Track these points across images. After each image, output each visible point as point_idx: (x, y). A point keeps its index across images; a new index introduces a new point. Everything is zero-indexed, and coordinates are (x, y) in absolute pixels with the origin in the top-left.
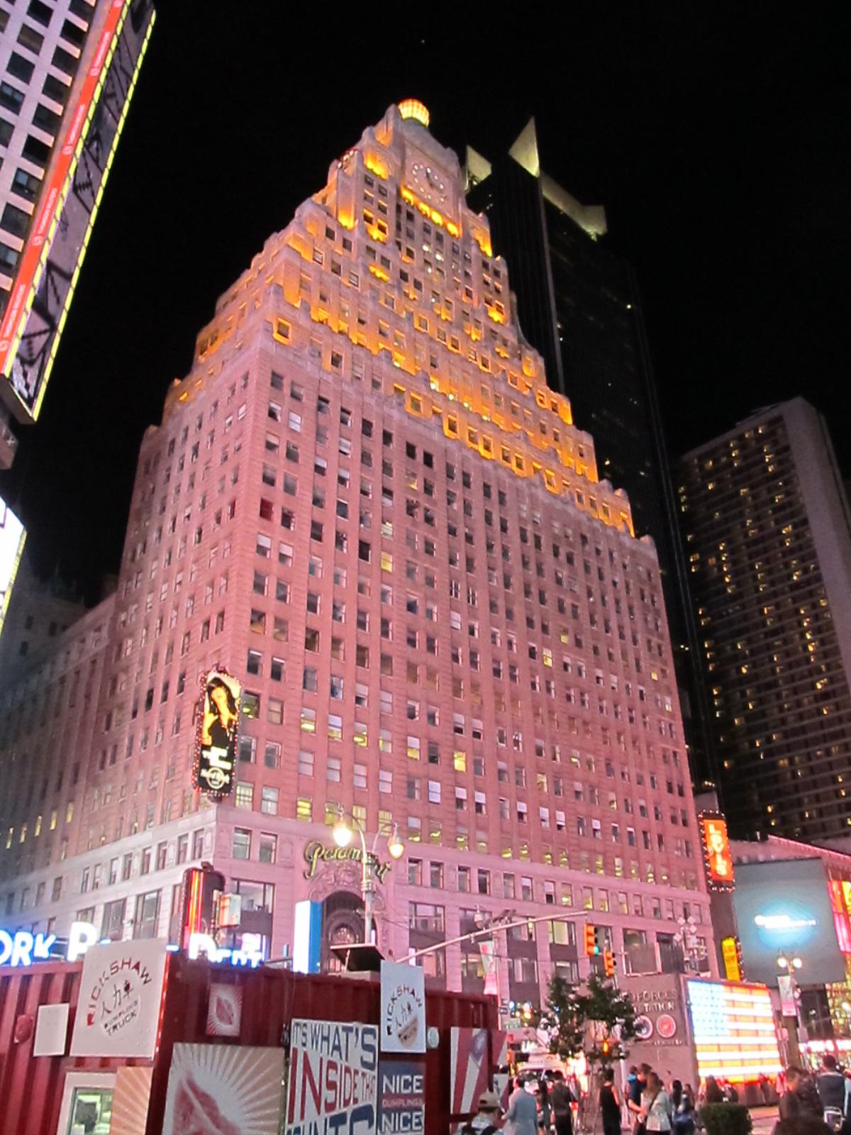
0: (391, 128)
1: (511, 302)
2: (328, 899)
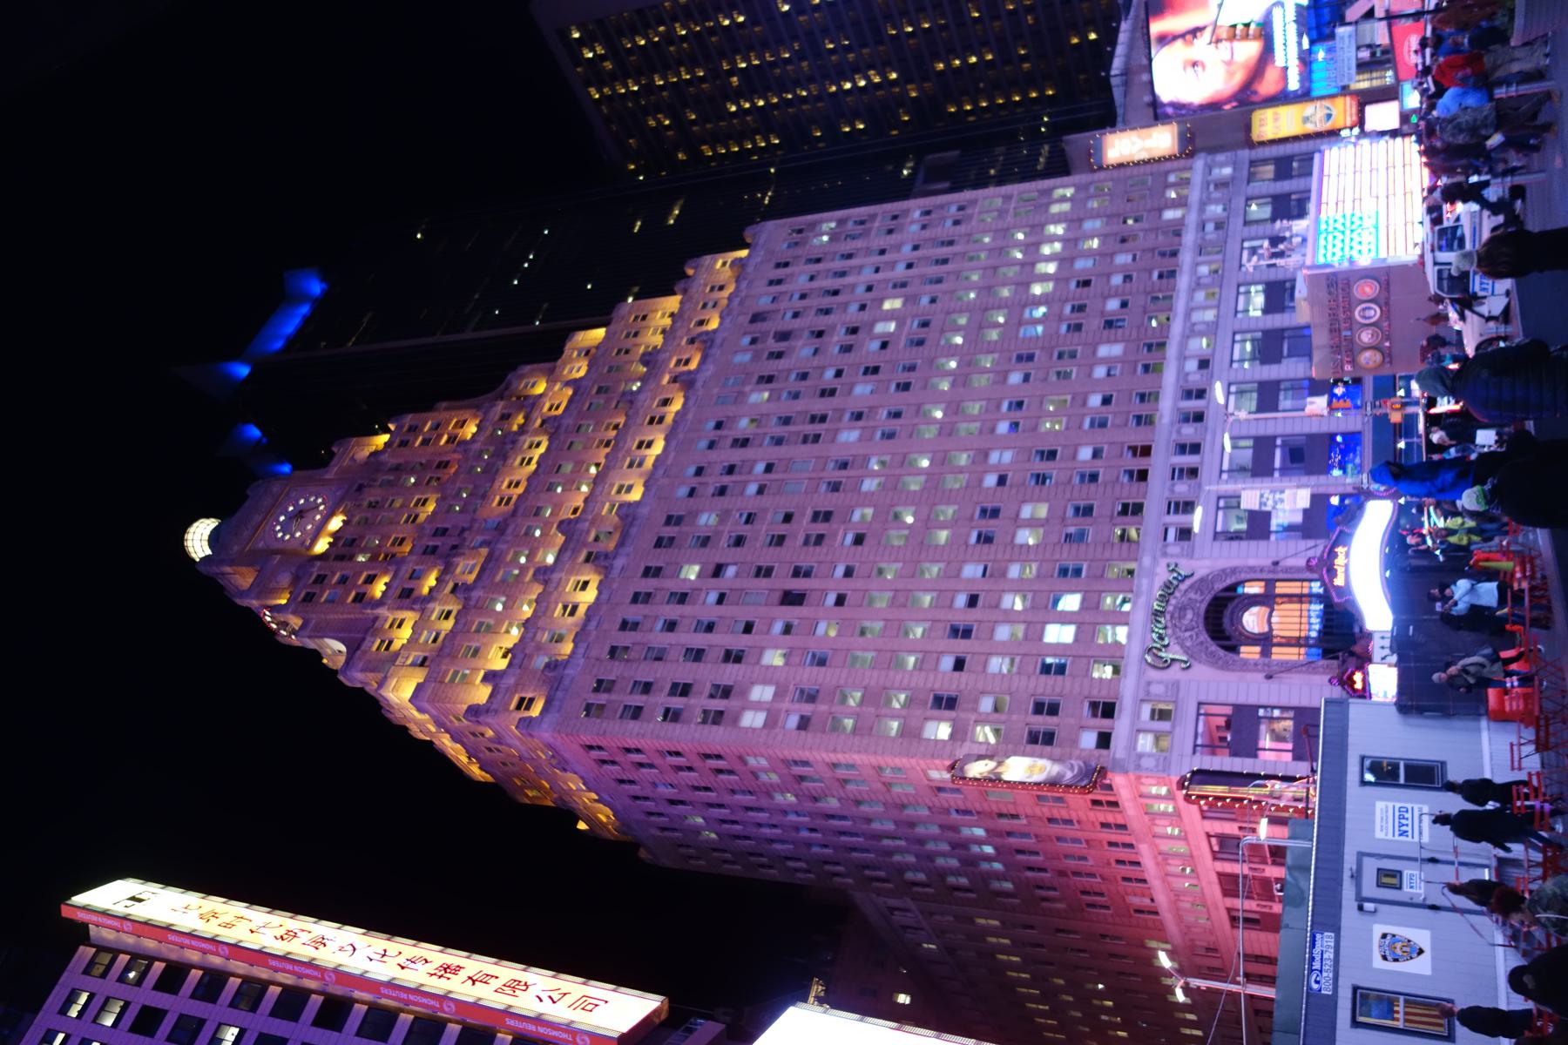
0: (228, 569)
1: (447, 409)
2: (1213, 638)
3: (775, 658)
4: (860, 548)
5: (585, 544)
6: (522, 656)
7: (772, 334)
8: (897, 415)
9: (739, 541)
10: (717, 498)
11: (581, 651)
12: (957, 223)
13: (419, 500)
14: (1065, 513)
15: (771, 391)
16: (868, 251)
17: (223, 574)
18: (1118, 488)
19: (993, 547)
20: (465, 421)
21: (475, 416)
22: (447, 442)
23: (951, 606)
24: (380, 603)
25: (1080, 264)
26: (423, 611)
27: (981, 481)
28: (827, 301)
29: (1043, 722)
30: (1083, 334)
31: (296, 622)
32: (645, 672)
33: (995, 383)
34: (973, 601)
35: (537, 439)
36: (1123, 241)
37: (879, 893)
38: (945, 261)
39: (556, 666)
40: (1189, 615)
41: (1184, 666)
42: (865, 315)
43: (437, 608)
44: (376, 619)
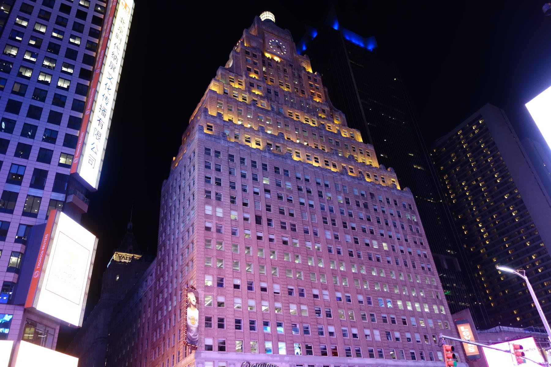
0: (256, 26)
1: (325, 91)
3: (234, 215)
4: (282, 243)
5: (274, 142)
6: (228, 125)
7: (366, 201)
8: (339, 253)
9: (280, 198)
10: (297, 187)
11: (231, 145)
12: (423, 268)
13: (289, 86)
14: (304, 323)
16: (405, 235)
17: (255, 25)
18: (318, 344)
19: (287, 295)
20: (321, 98)
21: (323, 101)
22: (312, 92)
23: (260, 281)
24: (247, 76)
25: (413, 319)
26: (246, 91)
27: (315, 288)
29: (215, 322)
30: (382, 323)
31: (238, 50)
33: (357, 290)
34: (264, 289)
35: (316, 123)
36: (425, 337)
37: (156, 269)
39: (224, 137)
42: (379, 236)
43: (246, 96)
44: (242, 76)
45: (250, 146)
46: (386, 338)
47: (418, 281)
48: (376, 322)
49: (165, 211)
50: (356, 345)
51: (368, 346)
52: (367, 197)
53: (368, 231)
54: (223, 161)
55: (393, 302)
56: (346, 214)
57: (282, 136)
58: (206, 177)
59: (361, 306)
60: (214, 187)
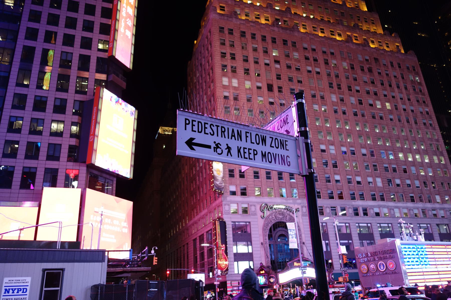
2: (274, 225)
3: (248, 85)
6: (239, 4)
7: (371, 66)
9: (289, 67)
10: (304, 57)
11: (242, 22)
12: (425, 124)
15: (348, 69)
16: (408, 95)
18: (325, 189)
25: (413, 169)
27: (322, 144)
28: (386, 84)
30: (384, 172)
32: (238, 44)
33: (361, 144)
36: (424, 183)
38: (408, 122)
39: (236, 15)
40: (281, 217)
41: (262, 216)
42: (382, 97)
45: (260, 22)
46: (388, 185)
47: (419, 136)
48: (379, 172)
49: (192, 87)
50: (360, 191)
51: (371, 191)
52: (371, 62)
53: (372, 93)
54: (235, 38)
55: (395, 154)
56: (351, 79)
57: (289, 11)
58: (222, 53)
59: (364, 158)
60: (229, 61)
